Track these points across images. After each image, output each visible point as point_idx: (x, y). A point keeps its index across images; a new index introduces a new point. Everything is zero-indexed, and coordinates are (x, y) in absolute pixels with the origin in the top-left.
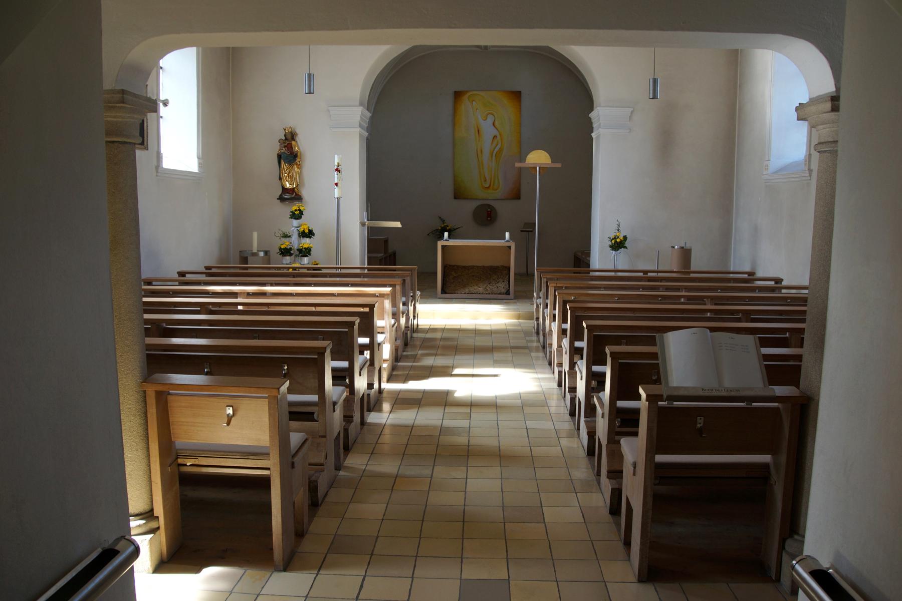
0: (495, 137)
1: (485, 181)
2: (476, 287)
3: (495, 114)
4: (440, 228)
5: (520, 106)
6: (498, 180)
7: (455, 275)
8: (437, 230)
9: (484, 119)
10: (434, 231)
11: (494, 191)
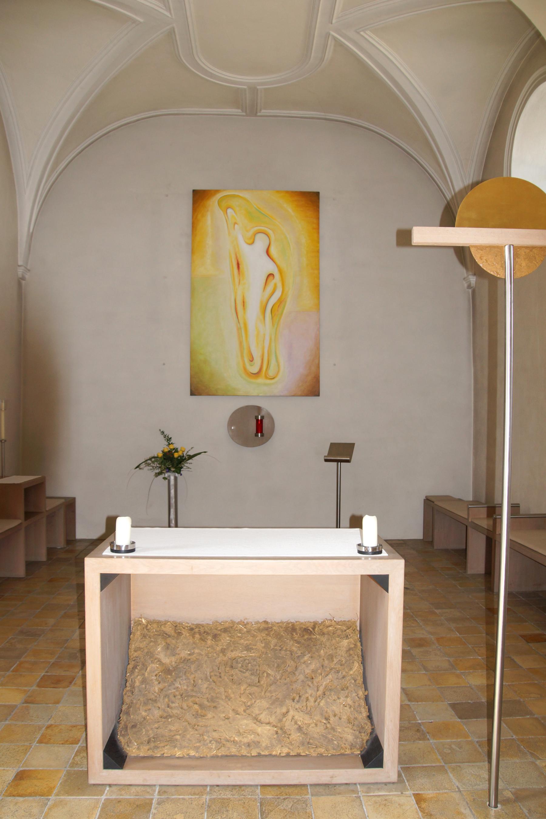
0: (271, 275)
1: (252, 360)
2: (246, 723)
3: (270, 232)
4: (161, 455)
5: (318, 219)
6: (277, 361)
7: (166, 660)
8: (154, 457)
10: (150, 459)
11: (268, 381)
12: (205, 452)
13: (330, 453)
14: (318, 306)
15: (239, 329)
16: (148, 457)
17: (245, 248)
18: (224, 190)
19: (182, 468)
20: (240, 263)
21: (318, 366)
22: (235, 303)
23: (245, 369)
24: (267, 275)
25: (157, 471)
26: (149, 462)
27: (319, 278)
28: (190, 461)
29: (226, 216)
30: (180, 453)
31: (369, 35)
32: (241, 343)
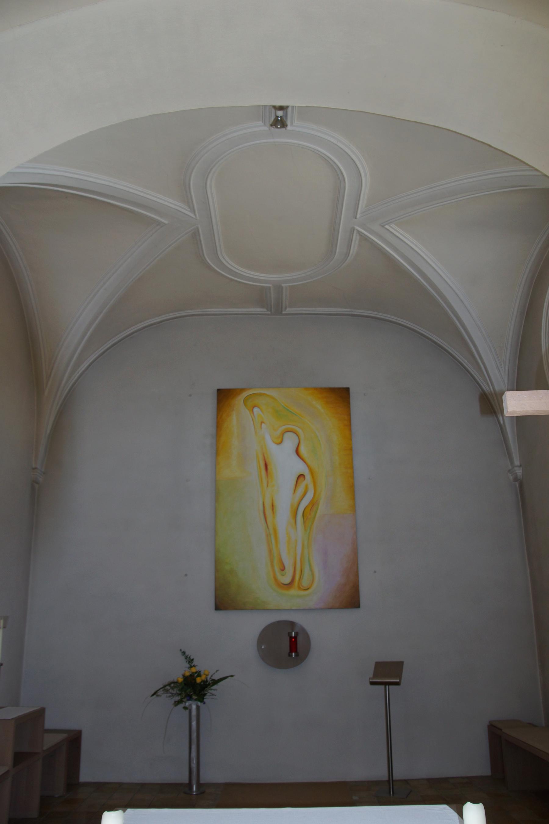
0: (301, 476)
1: (283, 569)
3: (299, 431)
4: (181, 680)
5: (349, 415)
6: (311, 570)
8: (173, 683)
9: (279, 441)
10: (169, 684)
11: (302, 593)
12: (232, 676)
13: (375, 675)
14: (354, 508)
15: (268, 535)
16: (166, 682)
17: (272, 447)
18: (250, 389)
19: (205, 695)
20: (268, 464)
21: (357, 575)
22: (264, 507)
23: (276, 579)
24: (297, 477)
25: (177, 698)
26: (168, 687)
27: (353, 477)
28: (215, 687)
29: (252, 415)
30: (203, 677)
31: (393, 228)
32: (270, 551)
